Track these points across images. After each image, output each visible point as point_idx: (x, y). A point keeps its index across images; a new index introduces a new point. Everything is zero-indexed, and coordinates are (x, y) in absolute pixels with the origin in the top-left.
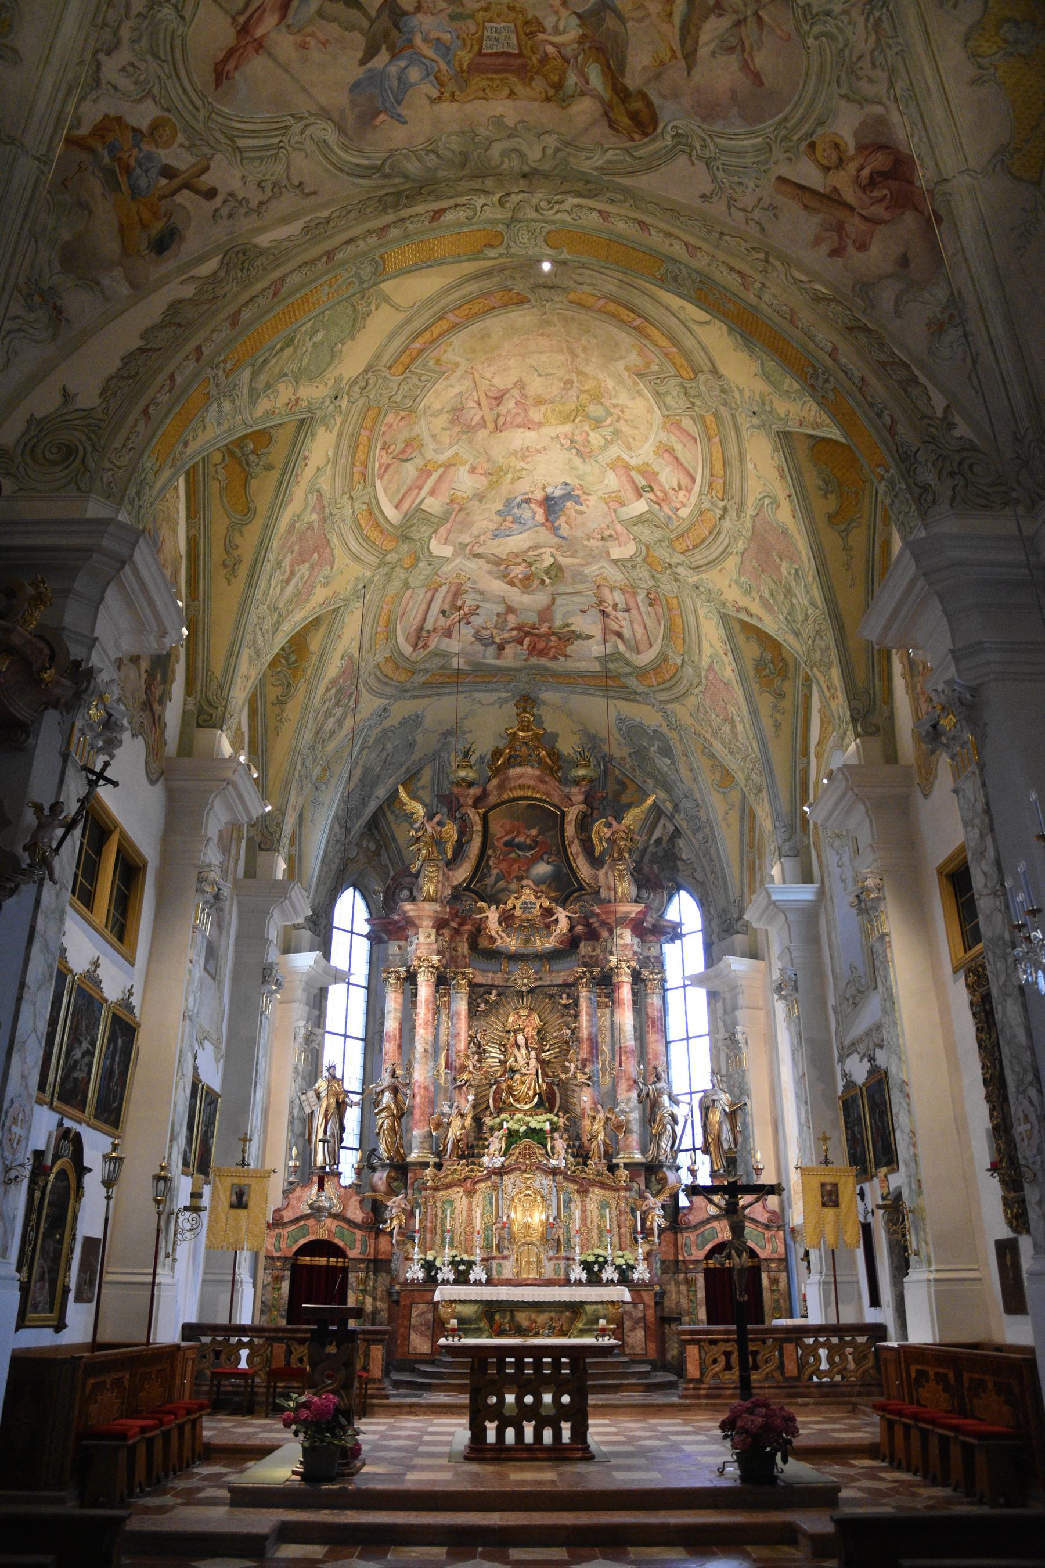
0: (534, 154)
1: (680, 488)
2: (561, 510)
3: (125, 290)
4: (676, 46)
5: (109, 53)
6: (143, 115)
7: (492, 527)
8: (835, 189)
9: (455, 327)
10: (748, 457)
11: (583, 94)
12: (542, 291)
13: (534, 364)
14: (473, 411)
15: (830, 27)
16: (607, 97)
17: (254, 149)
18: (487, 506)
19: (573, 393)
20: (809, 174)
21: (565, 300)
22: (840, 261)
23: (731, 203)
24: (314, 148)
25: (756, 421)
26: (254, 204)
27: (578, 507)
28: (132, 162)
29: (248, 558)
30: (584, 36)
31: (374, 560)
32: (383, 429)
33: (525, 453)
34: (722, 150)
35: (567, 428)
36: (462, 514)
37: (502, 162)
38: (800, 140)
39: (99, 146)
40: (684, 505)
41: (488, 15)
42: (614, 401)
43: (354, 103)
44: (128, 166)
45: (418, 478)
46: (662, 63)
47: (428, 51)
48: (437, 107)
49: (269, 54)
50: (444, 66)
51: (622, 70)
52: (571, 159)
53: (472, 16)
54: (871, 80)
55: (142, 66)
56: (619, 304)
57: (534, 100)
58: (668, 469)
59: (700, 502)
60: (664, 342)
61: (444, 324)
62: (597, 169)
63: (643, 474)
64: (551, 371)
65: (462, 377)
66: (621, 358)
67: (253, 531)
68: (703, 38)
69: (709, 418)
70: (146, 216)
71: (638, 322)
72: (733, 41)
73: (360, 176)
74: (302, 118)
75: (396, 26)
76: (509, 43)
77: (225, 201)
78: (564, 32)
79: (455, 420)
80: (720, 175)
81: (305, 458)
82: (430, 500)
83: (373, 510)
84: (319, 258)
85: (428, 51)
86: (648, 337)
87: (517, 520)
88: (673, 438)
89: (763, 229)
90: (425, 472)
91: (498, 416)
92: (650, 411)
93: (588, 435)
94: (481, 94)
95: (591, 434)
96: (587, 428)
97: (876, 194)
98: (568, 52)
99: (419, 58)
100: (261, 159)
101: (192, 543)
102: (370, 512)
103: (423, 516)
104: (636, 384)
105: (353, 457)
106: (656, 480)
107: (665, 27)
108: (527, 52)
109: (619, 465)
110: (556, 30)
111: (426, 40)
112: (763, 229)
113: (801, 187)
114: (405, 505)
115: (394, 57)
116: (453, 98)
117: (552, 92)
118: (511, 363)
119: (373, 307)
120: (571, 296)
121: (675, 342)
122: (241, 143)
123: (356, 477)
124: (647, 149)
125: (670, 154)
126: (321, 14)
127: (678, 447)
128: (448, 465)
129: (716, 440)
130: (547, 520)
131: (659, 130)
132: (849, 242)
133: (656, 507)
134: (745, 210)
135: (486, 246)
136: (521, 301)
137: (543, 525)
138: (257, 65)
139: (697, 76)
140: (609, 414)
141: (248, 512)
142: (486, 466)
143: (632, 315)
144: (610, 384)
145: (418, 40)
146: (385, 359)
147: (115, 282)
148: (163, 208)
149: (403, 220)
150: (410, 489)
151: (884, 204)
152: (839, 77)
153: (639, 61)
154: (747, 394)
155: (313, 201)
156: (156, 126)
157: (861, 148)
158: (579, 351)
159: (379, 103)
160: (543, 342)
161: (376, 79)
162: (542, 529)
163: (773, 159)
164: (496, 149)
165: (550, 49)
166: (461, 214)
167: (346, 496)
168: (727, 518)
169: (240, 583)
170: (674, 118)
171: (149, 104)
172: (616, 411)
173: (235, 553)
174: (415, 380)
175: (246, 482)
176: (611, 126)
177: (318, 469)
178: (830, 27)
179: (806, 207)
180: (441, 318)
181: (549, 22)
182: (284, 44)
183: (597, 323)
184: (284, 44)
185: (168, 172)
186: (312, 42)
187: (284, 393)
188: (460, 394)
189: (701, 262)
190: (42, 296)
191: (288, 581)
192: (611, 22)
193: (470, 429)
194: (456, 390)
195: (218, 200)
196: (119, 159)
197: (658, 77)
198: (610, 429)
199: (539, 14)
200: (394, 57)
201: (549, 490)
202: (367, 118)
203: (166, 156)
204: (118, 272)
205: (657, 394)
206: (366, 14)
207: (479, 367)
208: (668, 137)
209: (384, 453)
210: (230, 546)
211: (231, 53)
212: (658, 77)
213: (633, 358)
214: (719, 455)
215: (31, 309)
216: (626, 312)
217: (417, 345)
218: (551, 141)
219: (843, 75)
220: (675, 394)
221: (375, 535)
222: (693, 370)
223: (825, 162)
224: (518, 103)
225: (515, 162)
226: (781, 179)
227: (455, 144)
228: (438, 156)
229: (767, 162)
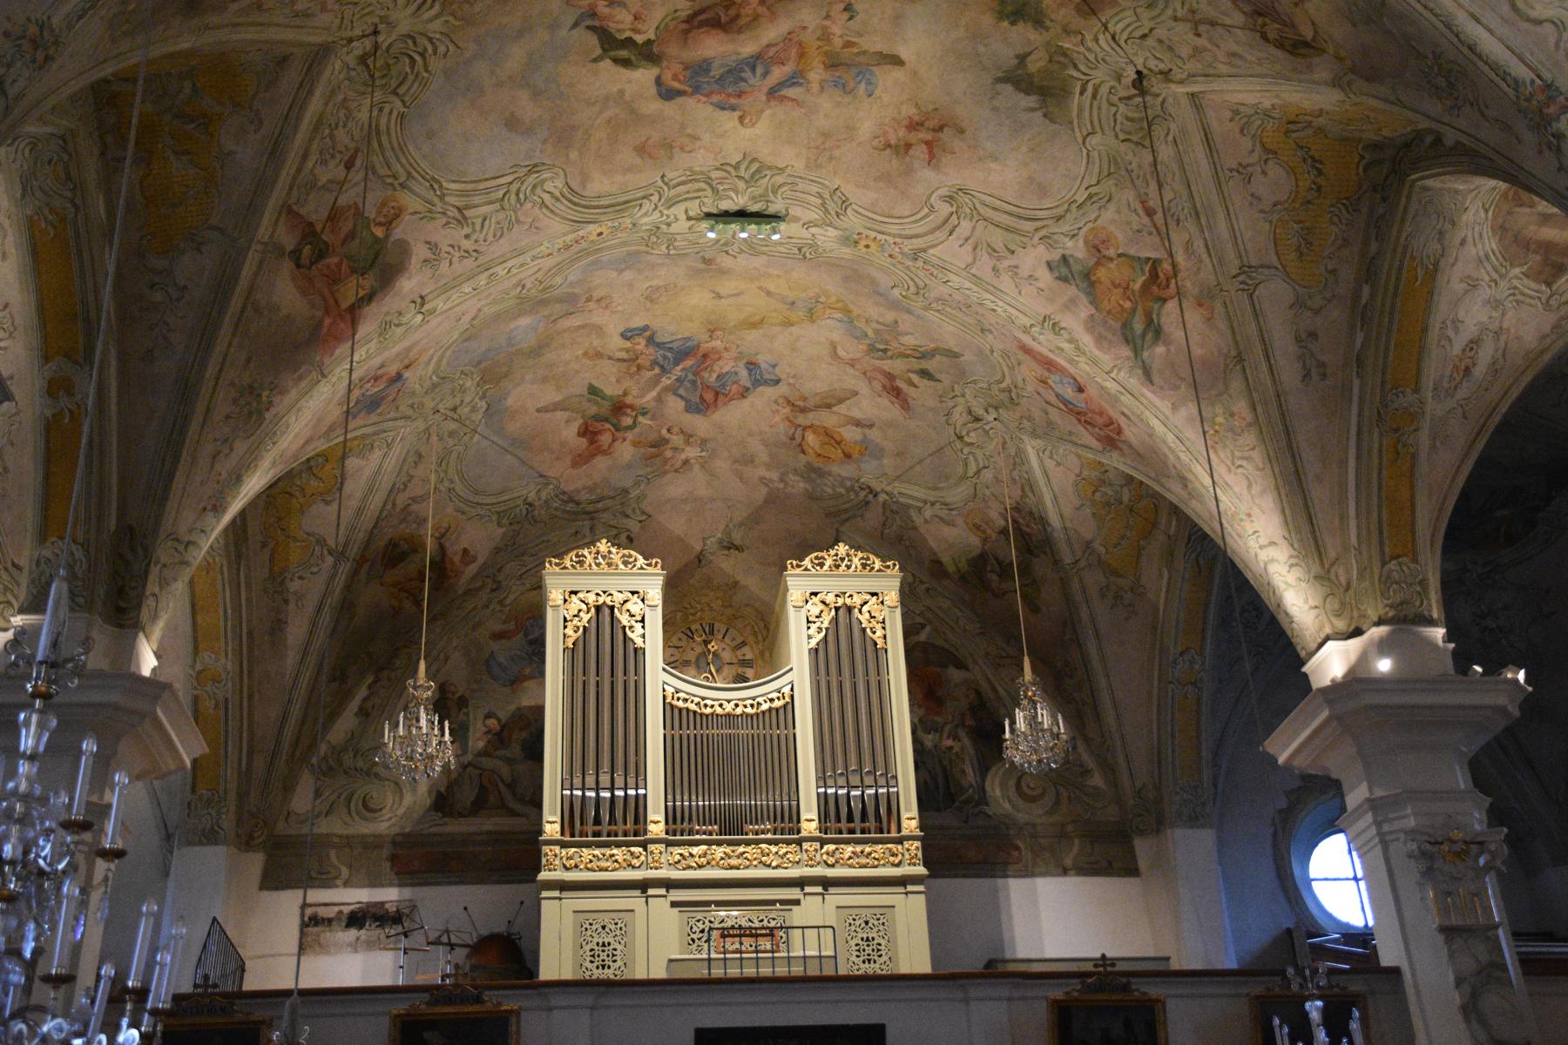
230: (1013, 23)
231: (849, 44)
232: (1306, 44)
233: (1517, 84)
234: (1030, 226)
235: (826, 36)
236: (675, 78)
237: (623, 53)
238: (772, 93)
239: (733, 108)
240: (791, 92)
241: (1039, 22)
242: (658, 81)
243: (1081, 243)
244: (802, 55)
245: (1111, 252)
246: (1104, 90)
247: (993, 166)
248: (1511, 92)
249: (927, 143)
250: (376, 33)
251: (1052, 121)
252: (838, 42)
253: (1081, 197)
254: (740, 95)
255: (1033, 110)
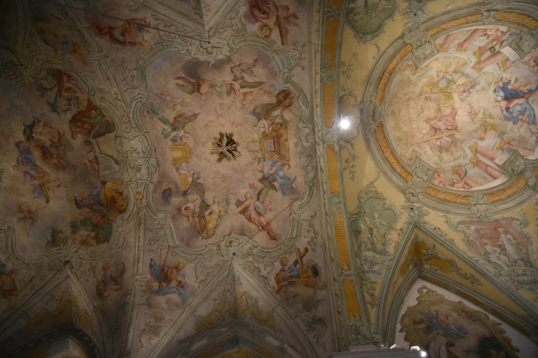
0: (307, 131)
1: (486, 34)
2: (514, 91)
3: (324, 292)
4: (258, 89)
5: (260, 272)
6: (278, 266)
7: (526, 125)
8: (275, 23)
9: (393, 153)
10: (444, 10)
11: (282, 116)
12: (376, 117)
13: (416, 115)
14: (442, 141)
15: (231, 42)
16: (282, 108)
17: (297, 231)
18: (509, 130)
19: (433, 96)
20: (275, 35)
21: (380, 107)
22: (298, 14)
23: (300, 59)
24: (301, 210)
25: (419, 13)
26: (314, 235)
27: (512, 82)
28: (289, 275)
29: (472, 271)
30: (264, 118)
31: (530, 192)
32: (441, 185)
33: (473, 114)
34: (284, 67)
35: (456, 96)
36: (512, 143)
37: (311, 142)
38: (267, 41)
39: (282, 284)
40: (498, 30)
41: (263, 149)
42: (435, 77)
43: (289, 195)
44: (290, 276)
45: (480, 167)
46: (265, 92)
47: (275, 168)
48: (291, 166)
49: (271, 221)
50: (279, 164)
51: (271, 105)
52: (306, 117)
53: (264, 155)
54: (237, 25)
55: (265, 262)
56: (379, 84)
57: (287, 132)
58: (474, 43)
59: (491, 23)
60: (395, 61)
61: (391, 158)
62: (307, 108)
63: (481, 54)
64: (420, 108)
65: (421, 148)
66: (408, 77)
67: (460, 264)
68: (252, 81)
69: (431, 32)
70: (305, 275)
71: (386, 74)
72: (249, 71)
73: (312, 195)
74: (291, 213)
75: (267, 179)
76: (270, 142)
77: (310, 246)
78: (264, 124)
79: (447, 150)
80: (292, 65)
81: (435, 229)
82: (497, 161)
83: (490, 193)
84: (326, 219)
85: (275, 168)
86: (394, 69)
87: (522, 113)
88: (452, 45)
89: (304, 45)
90: (477, 163)
91: (447, 129)
92: (437, 59)
93: (459, 85)
94: (287, 151)
95: (458, 83)
96: (455, 86)
97: (267, 9)
98: (270, 123)
99: (276, 172)
100: (301, 229)
101: (458, 293)
102: (492, 194)
103: (507, 164)
104: (422, 69)
105: (450, 202)
106: (484, 47)
107: (254, 93)
108: (272, 136)
109: (478, 66)
110: (264, 127)
111: (271, 170)
112: (304, 45)
113: (281, 36)
114: (496, 173)
115: (276, 180)
116: (288, 160)
117: (284, 127)
118: (415, 126)
119: (373, 189)
120: (378, 104)
121: (393, 57)
122: (294, 236)
123: (464, 201)
124: (294, 92)
125: (293, 83)
126: (262, 203)
127: (457, 42)
128: (476, 151)
129: (443, 26)
130: (523, 97)
131: (286, 89)
132: (289, 13)
133: (504, 43)
134: (301, 54)
135: (333, 150)
136: (381, 125)
137: (527, 99)
138: (274, 225)
139: (264, 80)
140: (444, 77)
141: (451, 262)
142: (480, 132)
143: (384, 77)
144: (425, 80)
145: (271, 172)
146: (401, 184)
147: (321, 294)
148: (306, 269)
149: (322, 183)
150: (486, 172)
151: (268, 6)
152: (242, 35)
153: (267, 99)
154: (406, 21)
155: (318, 213)
156: (282, 263)
157: (257, 21)
158: (408, 97)
159: (289, 186)
160: (403, 113)
161: (282, 186)
162: (530, 99)
163: (278, 48)
164: (306, 144)
165: (270, 129)
166: (322, 160)
167: (473, 207)
168: (494, 8)
169: (482, 280)
170: (281, 85)
171: (276, 264)
172: (441, 75)
173: (468, 276)
174: (418, 170)
175: (439, 258)
176: (291, 105)
177: (446, 222)
178: (231, 42)
179: (287, 33)
180: (387, 159)
181: (262, 130)
182: (269, 215)
183: (391, 91)
184: (269, 215)
185: (296, 263)
186: (270, 206)
187: (394, 236)
188: (431, 148)
189: (318, 68)
190: (313, 323)
191: (503, 249)
192: (258, 110)
193: (454, 142)
194: (428, 150)
195: (309, 248)
196: (287, 279)
197: (270, 92)
198: (454, 75)
199: (261, 133)
200: (276, 180)
201: (499, 99)
202: (293, 190)
203: (291, 263)
204: (318, 292)
205: (426, 58)
206: (264, 188)
207: (416, 141)
208: (288, 85)
209: (456, 185)
210: (465, 276)
211: (269, 233)
212: (270, 92)
213: (407, 73)
214: (452, 22)
215: (315, 330)
216: (382, 80)
217: (399, 169)
218: (301, 125)
219: (241, 34)
220: (423, 51)
221: (509, 192)
222: (405, 46)
223: (268, 31)
224: (289, 138)
225: (310, 137)
226: (283, 44)
227: (304, 159)
228: (308, 165)
229: (280, 51)
230: (70, 226)
231: (48, 188)
232: (102, 296)
233: (126, 346)
234: (10, 251)
235: (49, 182)
236: (23, 146)
237: (28, 131)
238: (26, 173)
239: (18, 163)
240: (28, 178)
241: (73, 232)
242: (21, 142)
243: (12, 268)
244: (41, 177)
245: (13, 276)
246: (61, 255)
247: (25, 236)
248: (123, 346)
249: (25, 217)
250: (22, 65)
251: (46, 245)
252: (48, 185)
253: (26, 262)
254: (23, 164)
255: (47, 239)
